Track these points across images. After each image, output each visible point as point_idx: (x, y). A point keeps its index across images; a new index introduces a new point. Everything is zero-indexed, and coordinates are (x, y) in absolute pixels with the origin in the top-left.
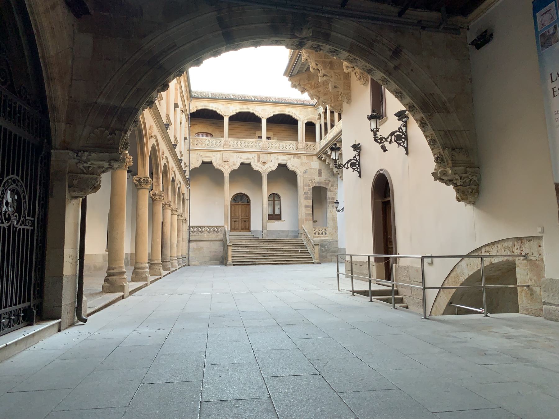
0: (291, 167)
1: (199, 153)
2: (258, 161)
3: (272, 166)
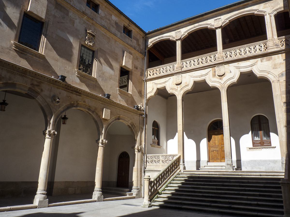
2: (214, 75)
3: (232, 78)
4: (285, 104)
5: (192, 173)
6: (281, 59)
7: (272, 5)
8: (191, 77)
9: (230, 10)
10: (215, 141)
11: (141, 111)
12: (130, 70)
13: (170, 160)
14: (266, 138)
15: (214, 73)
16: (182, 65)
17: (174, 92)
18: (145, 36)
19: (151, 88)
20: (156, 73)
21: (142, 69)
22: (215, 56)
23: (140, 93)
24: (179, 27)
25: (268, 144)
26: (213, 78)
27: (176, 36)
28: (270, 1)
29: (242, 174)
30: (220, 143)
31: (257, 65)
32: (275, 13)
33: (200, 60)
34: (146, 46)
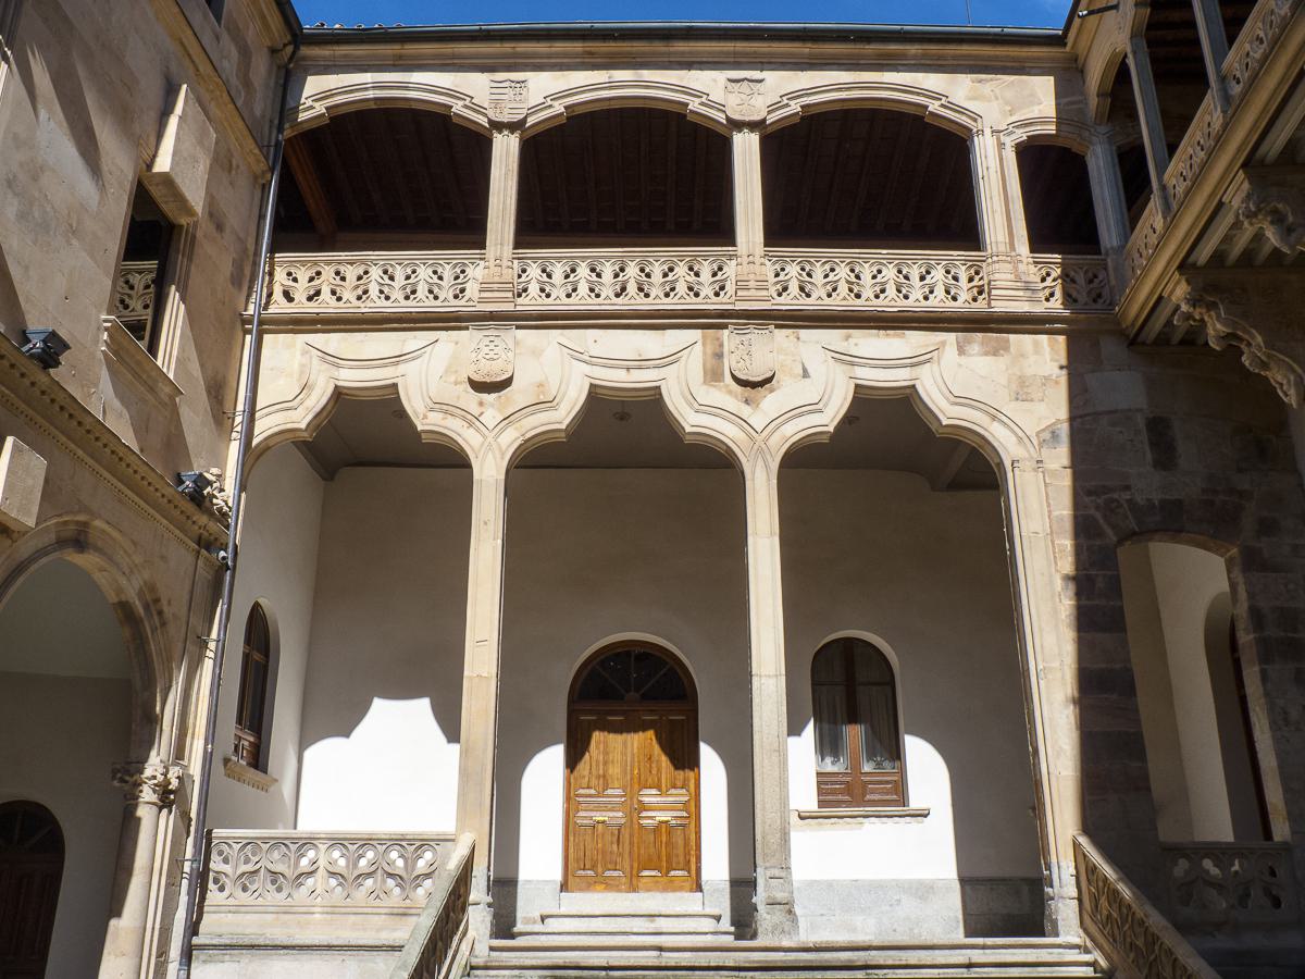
0: (946, 411)
1: (318, 339)
2: (713, 375)
3: (814, 408)
4: (1072, 587)
5: (560, 962)
6: (1045, 356)
7: (1009, 94)
8: (577, 355)
9: (811, 56)
10: (605, 763)
11: (211, 514)
12: (183, 221)
13: (390, 875)
14: (879, 765)
15: (711, 362)
16: (520, 276)
17: (460, 431)
18: (285, 45)
19: (291, 382)
20: (333, 293)
21: (239, 239)
22: (720, 269)
23: (216, 397)
24: (515, 55)
25: (895, 797)
26: (705, 387)
27: (496, 103)
28: (999, 76)
29: (869, 963)
30: (631, 779)
31: (939, 364)
32: (1021, 135)
33: (632, 270)
34: (288, 107)
